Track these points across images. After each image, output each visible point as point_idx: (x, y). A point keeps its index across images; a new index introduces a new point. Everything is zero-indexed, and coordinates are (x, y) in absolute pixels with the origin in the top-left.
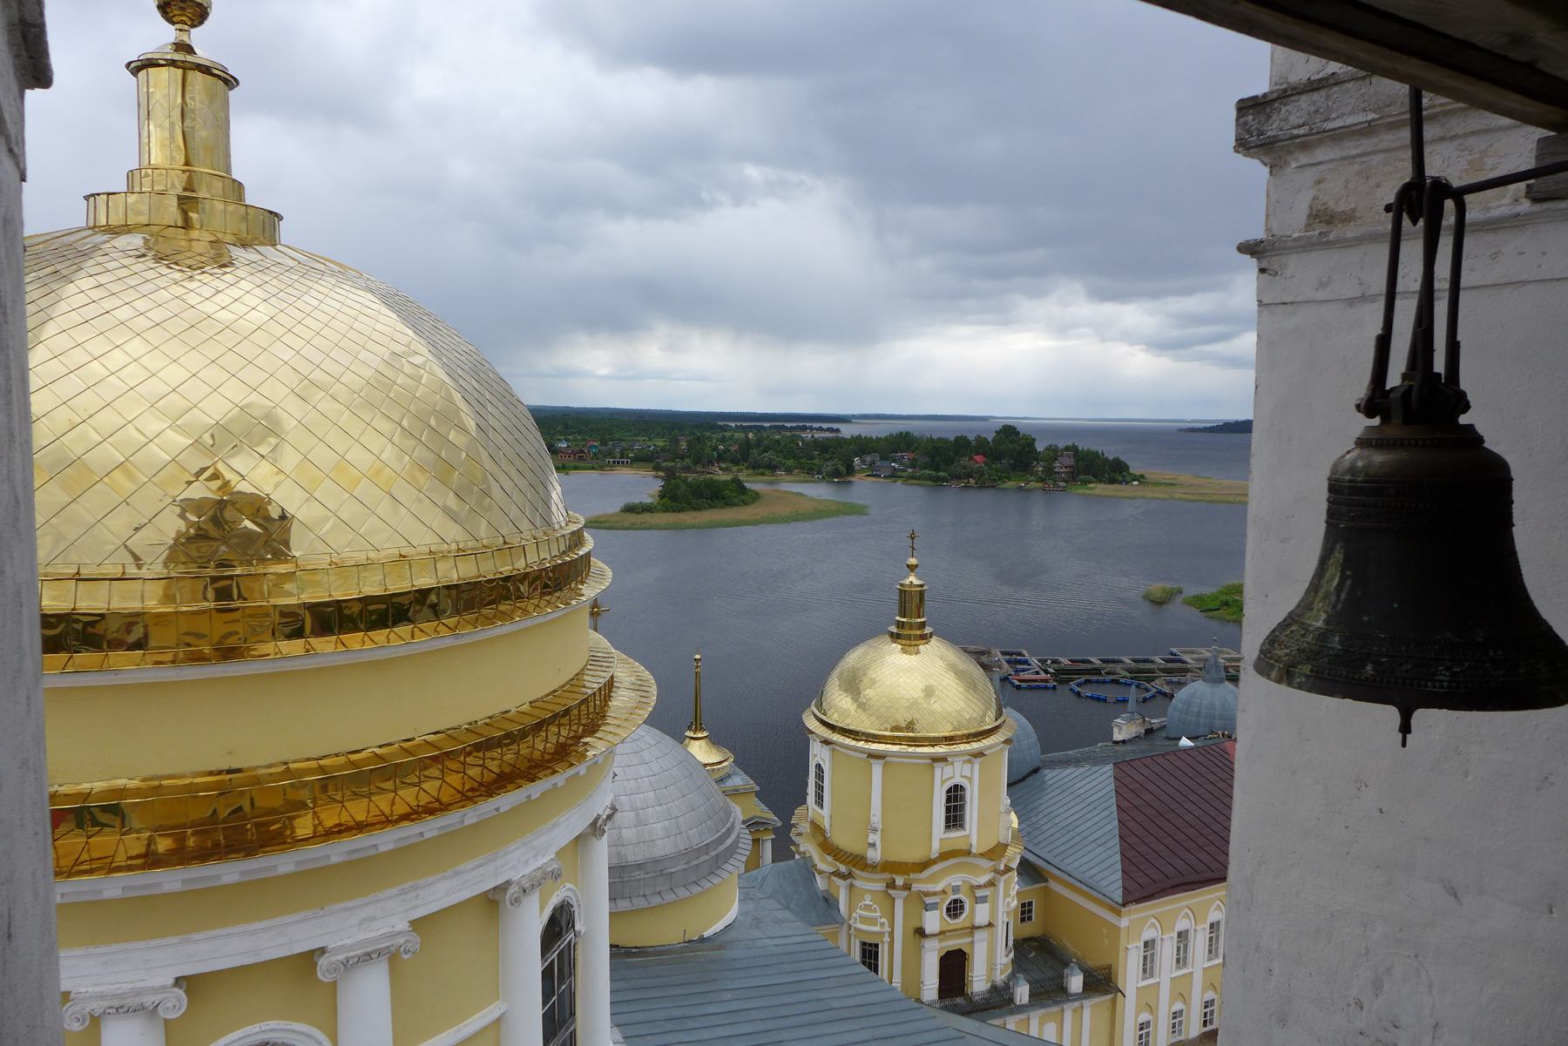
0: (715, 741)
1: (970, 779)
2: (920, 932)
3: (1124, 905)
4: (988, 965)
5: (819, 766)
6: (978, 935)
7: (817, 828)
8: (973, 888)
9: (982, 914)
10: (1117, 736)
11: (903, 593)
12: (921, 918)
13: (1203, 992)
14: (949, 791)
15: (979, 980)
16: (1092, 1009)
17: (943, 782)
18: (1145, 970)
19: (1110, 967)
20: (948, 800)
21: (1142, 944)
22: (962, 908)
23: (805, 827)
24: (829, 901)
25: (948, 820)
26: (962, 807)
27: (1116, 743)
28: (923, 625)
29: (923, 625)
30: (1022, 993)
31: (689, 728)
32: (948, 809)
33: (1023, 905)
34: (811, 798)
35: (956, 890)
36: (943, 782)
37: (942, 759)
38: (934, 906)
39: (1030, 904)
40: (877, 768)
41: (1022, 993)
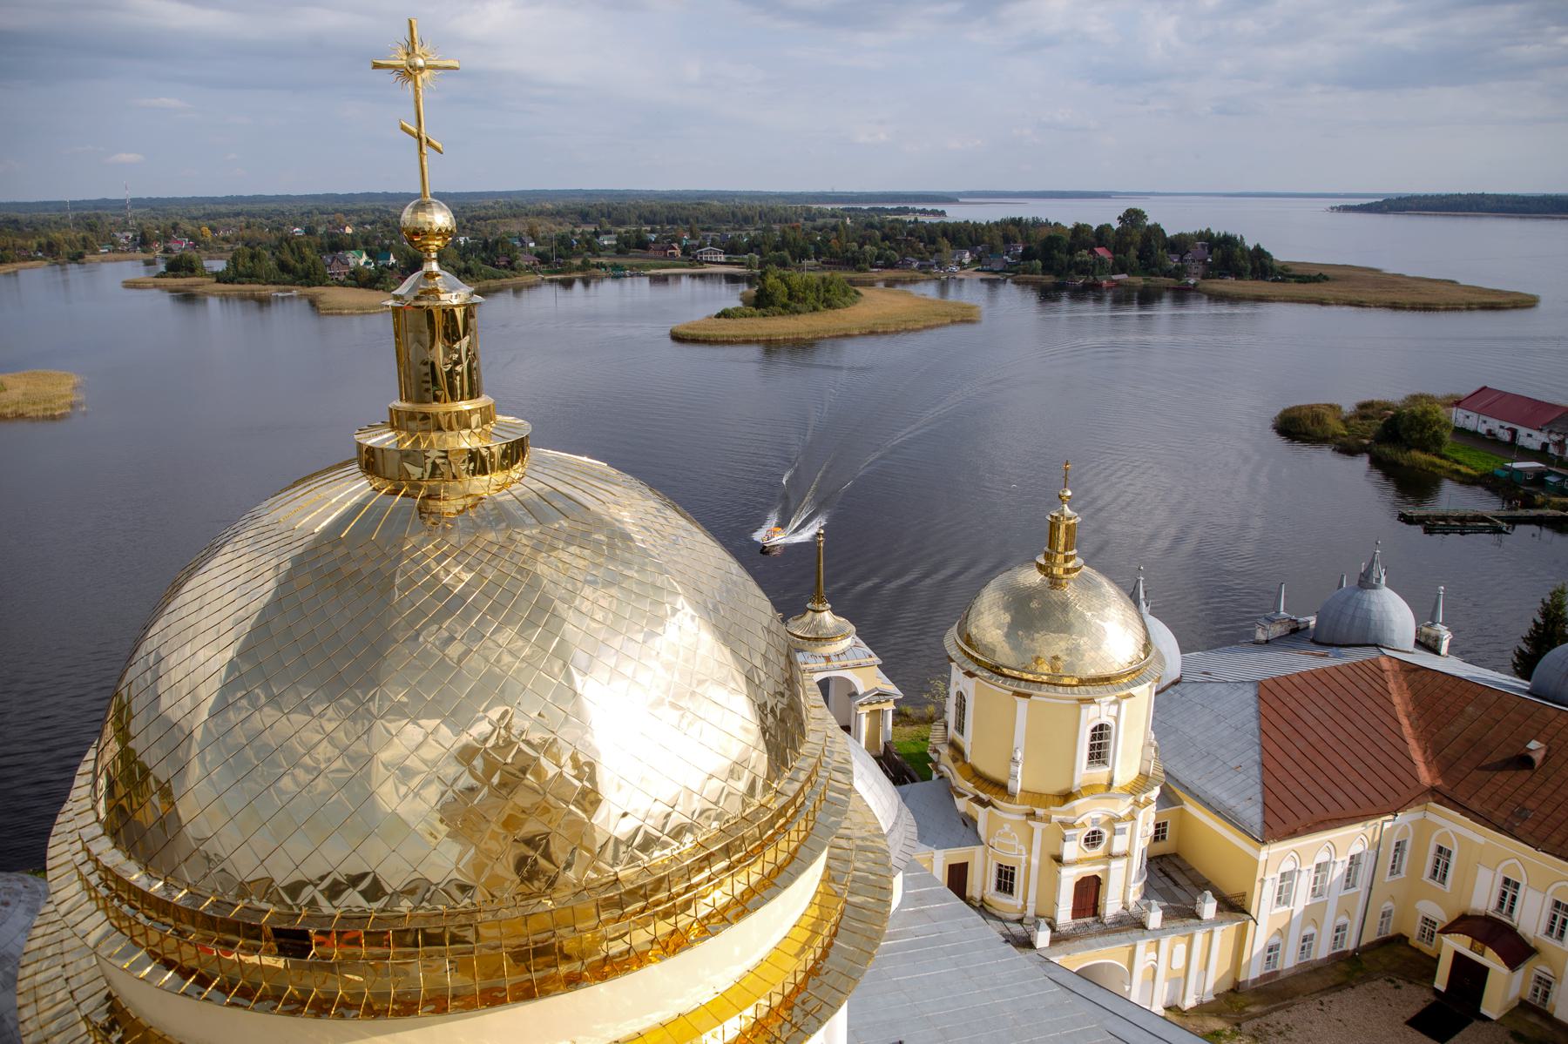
0: (835, 612)
1: (1117, 719)
2: (1058, 859)
3: (1264, 843)
4: (1123, 889)
5: (961, 696)
6: (1115, 864)
7: (957, 751)
8: (1113, 821)
9: (1119, 844)
10: (1260, 636)
11: (1052, 524)
12: (1059, 847)
13: (1337, 916)
14: (1095, 729)
15: (1112, 906)
16: (1224, 934)
18: (1279, 899)
19: (1244, 895)
20: (1093, 738)
21: (1278, 876)
22: (1100, 838)
23: (945, 751)
24: (969, 822)
25: (1091, 757)
27: (1257, 643)
29: (1072, 557)
30: (1155, 919)
32: (1092, 747)
33: (1157, 826)
35: (1095, 821)
38: (1073, 838)
39: (1165, 824)
40: (1022, 703)
41: (1155, 919)
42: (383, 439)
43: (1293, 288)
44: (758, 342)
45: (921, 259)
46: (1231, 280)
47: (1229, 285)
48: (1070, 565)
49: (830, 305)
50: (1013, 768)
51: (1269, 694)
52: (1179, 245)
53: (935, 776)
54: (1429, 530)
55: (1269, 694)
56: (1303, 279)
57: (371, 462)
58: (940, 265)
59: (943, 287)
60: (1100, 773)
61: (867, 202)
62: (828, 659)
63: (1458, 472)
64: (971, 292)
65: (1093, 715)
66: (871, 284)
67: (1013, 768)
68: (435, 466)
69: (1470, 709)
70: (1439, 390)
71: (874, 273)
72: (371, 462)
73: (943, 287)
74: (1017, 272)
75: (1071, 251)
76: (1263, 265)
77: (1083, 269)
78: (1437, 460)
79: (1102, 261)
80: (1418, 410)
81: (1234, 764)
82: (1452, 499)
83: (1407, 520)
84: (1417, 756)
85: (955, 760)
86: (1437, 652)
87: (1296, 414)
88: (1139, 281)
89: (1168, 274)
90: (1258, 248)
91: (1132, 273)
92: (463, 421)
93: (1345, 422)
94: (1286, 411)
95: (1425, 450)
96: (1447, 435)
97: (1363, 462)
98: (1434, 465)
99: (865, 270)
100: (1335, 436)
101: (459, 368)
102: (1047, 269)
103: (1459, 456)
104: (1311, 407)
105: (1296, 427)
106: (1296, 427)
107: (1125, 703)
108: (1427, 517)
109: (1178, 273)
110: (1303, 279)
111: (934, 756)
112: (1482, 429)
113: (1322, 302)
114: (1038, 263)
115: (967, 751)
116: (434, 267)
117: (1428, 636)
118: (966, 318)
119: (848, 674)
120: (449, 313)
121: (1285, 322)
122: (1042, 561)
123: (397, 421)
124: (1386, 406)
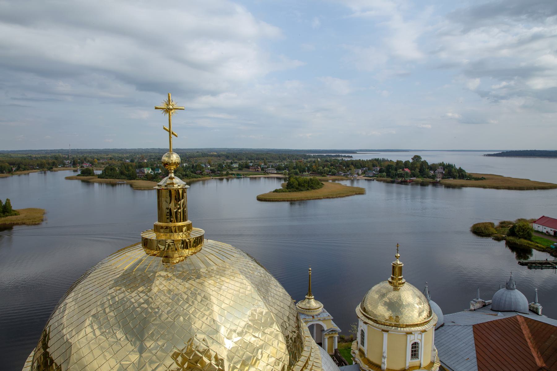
1: (421, 340)
5: (362, 331)
7: (362, 353)
10: (472, 308)
11: (393, 267)
14: (413, 344)
17: (410, 341)
20: (412, 348)
23: (357, 352)
25: (412, 355)
26: (418, 351)
27: (471, 310)
28: (401, 279)
29: (401, 279)
31: (307, 295)
32: (412, 351)
34: (359, 339)
36: (410, 341)
37: (411, 333)
40: (385, 335)
42: (152, 236)
43: (473, 182)
44: (288, 201)
45: (344, 172)
46: (452, 179)
47: (451, 181)
48: (400, 282)
49: (313, 188)
50: (383, 360)
51: (478, 329)
52: (433, 167)
53: (354, 363)
54: (530, 268)
55: (478, 329)
56: (477, 179)
57: (146, 243)
58: (351, 174)
59: (352, 181)
60: (416, 362)
61: (325, 153)
62: (313, 317)
63: (537, 246)
64: (362, 184)
65: (411, 339)
66: (327, 181)
67: (383, 360)
68: (169, 245)
69: (553, 336)
70: (528, 218)
71: (328, 177)
72: (146, 243)
73: (352, 181)
74: (378, 177)
75: (396, 170)
76: (462, 174)
77: (401, 176)
78: (529, 242)
79: (407, 173)
80: (521, 224)
81: (466, 358)
82: (537, 256)
83: (522, 264)
84: (535, 354)
85: (361, 356)
86: (537, 314)
87: (478, 226)
88: (420, 180)
89: (430, 177)
90: (460, 168)
91: (418, 177)
92: (180, 229)
93: (496, 229)
94: (475, 225)
95: (525, 238)
96: (533, 234)
97: (504, 242)
98: (528, 243)
99: (325, 176)
100: (493, 233)
101: (179, 211)
102: (388, 176)
103: (538, 241)
104: (483, 223)
105: (479, 231)
106: (479, 231)
107: (423, 334)
108: (528, 263)
109: (434, 177)
110: (477, 179)
111: (353, 355)
112: (545, 231)
113: (484, 187)
114: (385, 174)
115: (366, 353)
116: (173, 175)
117: (533, 308)
118: (361, 192)
119: (321, 323)
120: (177, 191)
121: (471, 193)
122: (390, 279)
123: (157, 229)
124: (510, 223)
